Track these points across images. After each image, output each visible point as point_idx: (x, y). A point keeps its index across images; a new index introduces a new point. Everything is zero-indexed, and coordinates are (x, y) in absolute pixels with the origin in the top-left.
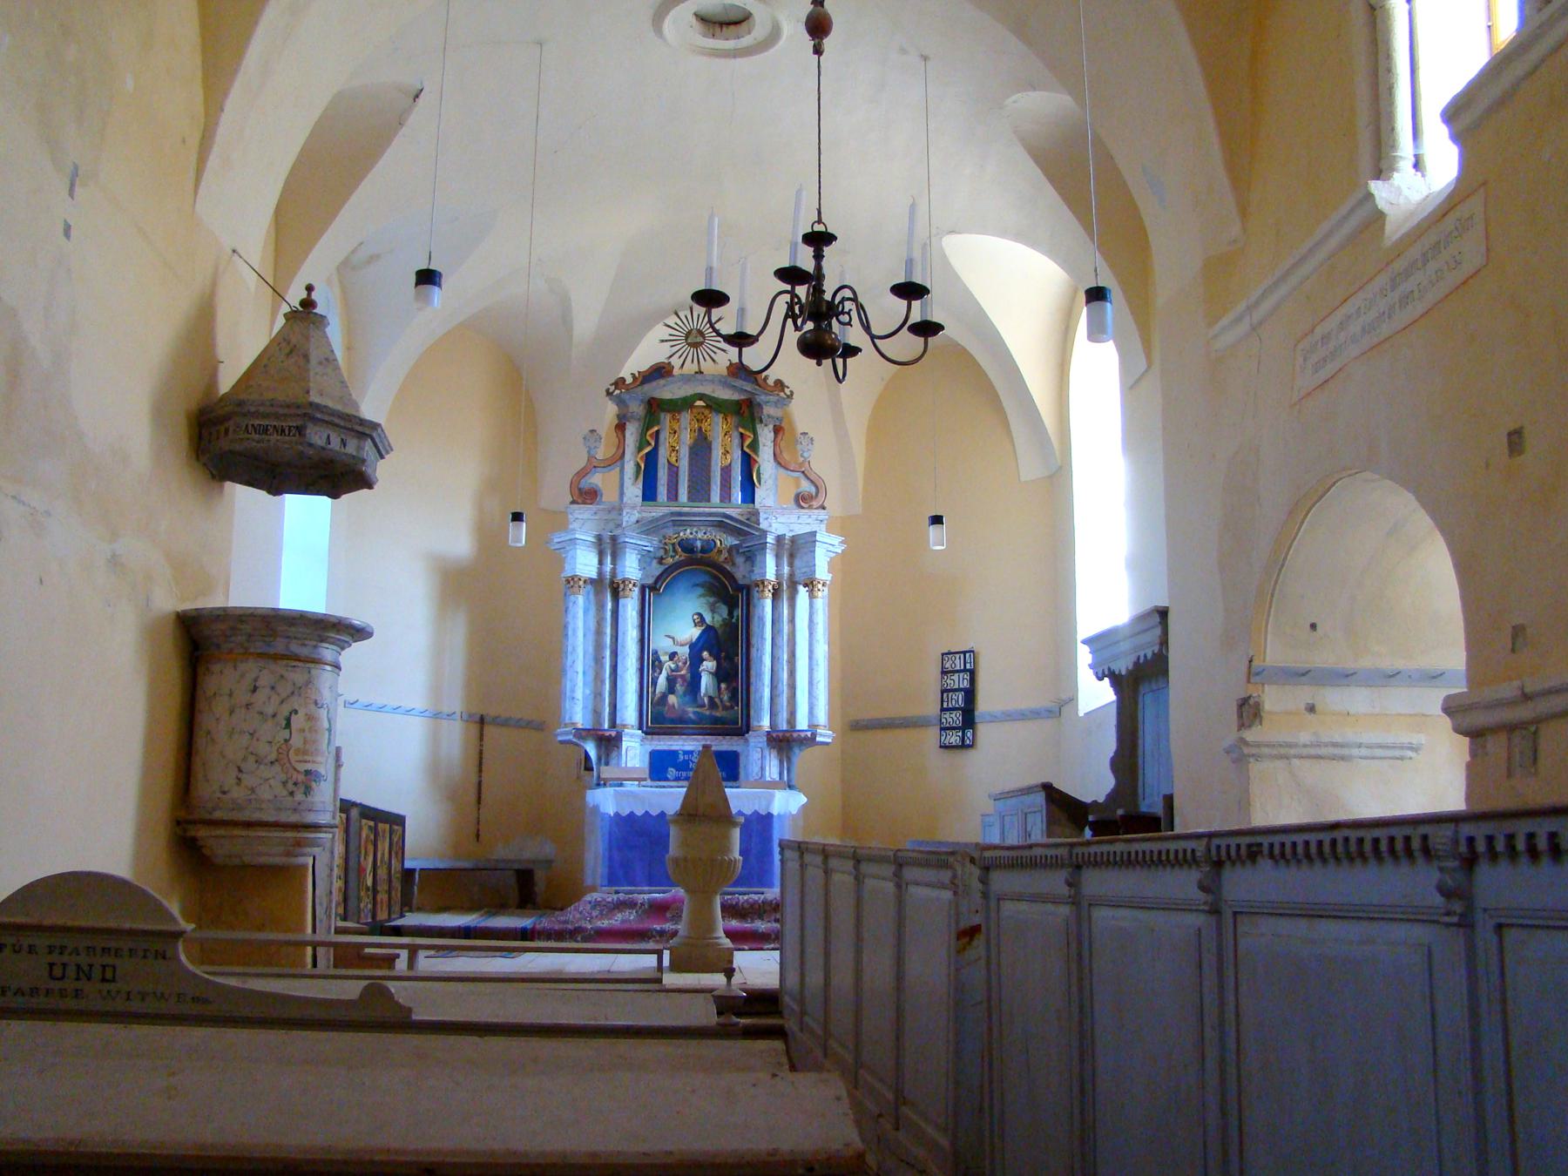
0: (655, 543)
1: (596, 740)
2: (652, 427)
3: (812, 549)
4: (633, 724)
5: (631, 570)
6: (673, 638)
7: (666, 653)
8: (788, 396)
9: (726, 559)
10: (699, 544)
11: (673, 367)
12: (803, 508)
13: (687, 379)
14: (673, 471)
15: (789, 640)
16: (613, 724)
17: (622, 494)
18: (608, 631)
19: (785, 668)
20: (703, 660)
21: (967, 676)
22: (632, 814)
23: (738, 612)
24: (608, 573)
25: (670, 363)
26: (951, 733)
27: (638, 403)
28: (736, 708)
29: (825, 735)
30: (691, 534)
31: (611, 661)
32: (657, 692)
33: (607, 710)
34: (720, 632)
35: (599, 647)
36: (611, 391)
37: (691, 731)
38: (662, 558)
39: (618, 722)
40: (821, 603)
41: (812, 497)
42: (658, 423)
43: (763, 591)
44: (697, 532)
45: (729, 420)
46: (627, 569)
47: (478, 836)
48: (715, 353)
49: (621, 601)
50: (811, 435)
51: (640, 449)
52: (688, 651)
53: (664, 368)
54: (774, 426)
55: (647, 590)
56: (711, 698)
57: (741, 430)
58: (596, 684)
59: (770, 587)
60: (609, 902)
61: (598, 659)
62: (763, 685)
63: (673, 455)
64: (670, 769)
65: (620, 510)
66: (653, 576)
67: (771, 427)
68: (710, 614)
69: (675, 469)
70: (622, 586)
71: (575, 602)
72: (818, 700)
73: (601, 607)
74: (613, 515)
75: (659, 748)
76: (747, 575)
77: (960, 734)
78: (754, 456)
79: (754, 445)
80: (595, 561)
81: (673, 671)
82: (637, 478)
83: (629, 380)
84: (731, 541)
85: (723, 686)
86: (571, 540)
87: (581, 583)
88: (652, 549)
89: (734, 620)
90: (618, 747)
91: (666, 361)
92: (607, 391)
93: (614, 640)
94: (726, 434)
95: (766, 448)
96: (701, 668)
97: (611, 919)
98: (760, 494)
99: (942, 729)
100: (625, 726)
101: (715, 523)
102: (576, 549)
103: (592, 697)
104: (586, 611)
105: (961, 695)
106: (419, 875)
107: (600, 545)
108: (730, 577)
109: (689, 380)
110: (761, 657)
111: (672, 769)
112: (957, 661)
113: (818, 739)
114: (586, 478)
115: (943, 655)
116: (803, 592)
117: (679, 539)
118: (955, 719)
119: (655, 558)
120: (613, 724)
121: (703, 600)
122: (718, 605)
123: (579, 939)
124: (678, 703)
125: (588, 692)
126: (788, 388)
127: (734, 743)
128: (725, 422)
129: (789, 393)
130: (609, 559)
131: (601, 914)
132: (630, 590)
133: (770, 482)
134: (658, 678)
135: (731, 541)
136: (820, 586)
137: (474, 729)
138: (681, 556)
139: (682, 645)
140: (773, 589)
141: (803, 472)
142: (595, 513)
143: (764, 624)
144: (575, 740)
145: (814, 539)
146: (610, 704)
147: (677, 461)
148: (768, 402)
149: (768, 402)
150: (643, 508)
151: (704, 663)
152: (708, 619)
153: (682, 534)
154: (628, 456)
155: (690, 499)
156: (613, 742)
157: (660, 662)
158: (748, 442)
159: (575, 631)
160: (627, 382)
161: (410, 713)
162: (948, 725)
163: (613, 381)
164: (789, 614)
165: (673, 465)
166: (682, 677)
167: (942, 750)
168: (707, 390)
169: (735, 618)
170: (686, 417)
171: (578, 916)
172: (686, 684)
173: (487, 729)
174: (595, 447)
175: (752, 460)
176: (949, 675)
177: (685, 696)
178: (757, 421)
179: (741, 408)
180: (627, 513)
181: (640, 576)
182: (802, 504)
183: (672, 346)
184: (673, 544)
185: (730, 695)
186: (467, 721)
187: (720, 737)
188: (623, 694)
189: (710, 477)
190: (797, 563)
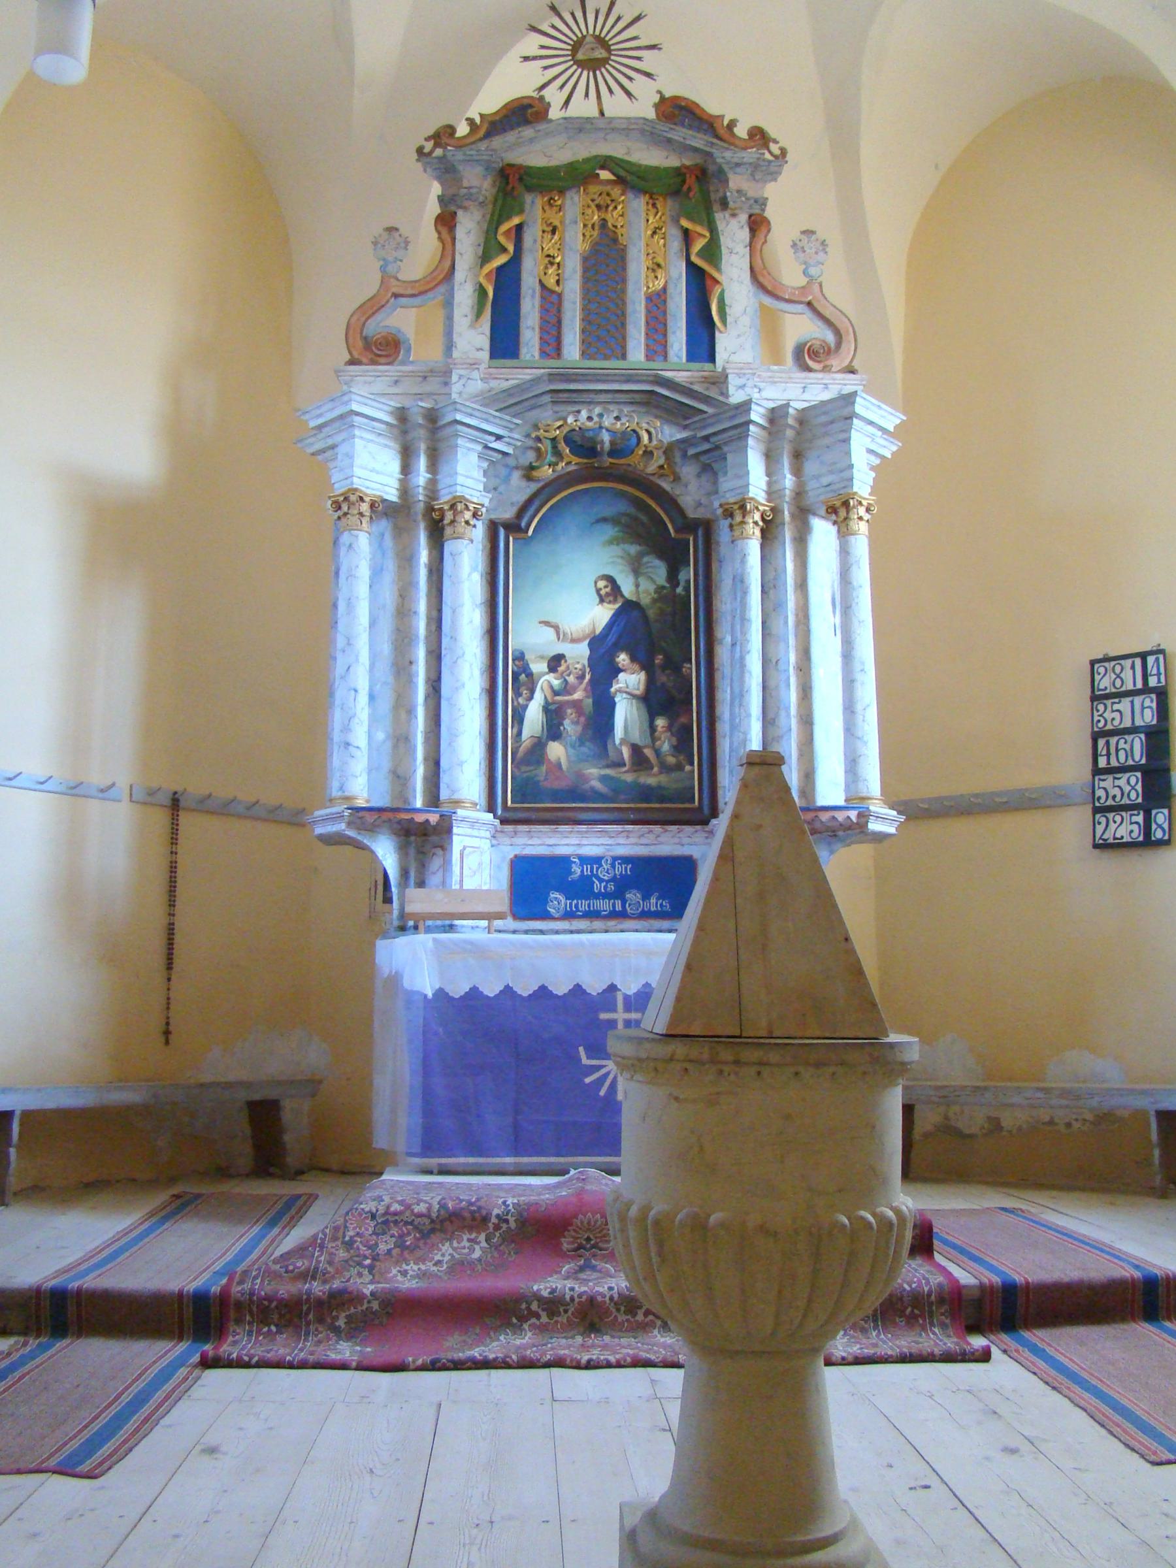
0: (516, 436)
1: (395, 833)
2: (509, 218)
3: (842, 436)
4: (476, 798)
5: (469, 483)
6: (556, 628)
7: (542, 657)
8: (776, 157)
9: (661, 467)
10: (606, 437)
11: (549, 104)
12: (809, 370)
13: (579, 127)
14: (552, 301)
15: (798, 624)
16: (433, 799)
17: (449, 347)
18: (422, 606)
19: (793, 680)
20: (620, 670)
21: (1150, 702)
22: (474, 993)
23: (688, 574)
24: (421, 490)
25: (542, 98)
26: (1118, 819)
27: (479, 169)
28: (688, 768)
29: (885, 821)
30: (590, 418)
31: (428, 670)
32: (526, 733)
33: (420, 771)
34: (651, 613)
35: (402, 639)
36: (426, 150)
37: (597, 816)
38: (532, 468)
39: (444, 794)
40: (861, 546)
41: (829, 349)
42: (521, 211)
43: (743, 523)
44: (601, 416)
45: (658, 206)
46: (460, 480)
47: (167, 1033)
48: (630, 79)
49: (449, 547)
50: (821, 235)
51: (485, 259)
52: (587, 652)
53: (531, 106)
54: (750, 216)
55: (502, 532)
56: (636, 750)
57: (685, 223)
58: (396, 720)
59: (757, 516)
60: (420, 1215)
61: (402, 668)
62: (749, 716)
63: (550, 271)
64: (554, 895)
65: (447, 373)
66: (512, 504)
67: (743, 218)
69: (555, 297)
70: (449, 516)
71: (350, 546)
72: (866, 743)
73: (406, 560)
74: (433, 385)
75: (529, 851)
77: (1140, 818)
78: (715, 274)
79: (712, 251)
80: (395, 466)
81: (556, 693)
82: (479, 314)
83: (462, 130)
84: (669, 433)
85: (660, 722)
86: (342, 417)
87: (365, 507)
88: (510, 451)
89: (679, 590)
90: (442, 848)
91: (535, 95)
92: (420, 151)
93: (434, 628)
94: (654, 233)
96: (613, 690)
97: (422, 1260)
98: (725, 344)
99: (1096, 810)
100: (457, 803)
101: (638, 397)
102: (353, 437)
103: (389, 745)
104: (376, 573)
105: (1138, 744)
106: (22, 1125)
107: (405, 432)
108: (671, 503)
109: (580, 130)
110: (742, 659)
111: (557, 895)
112: (1127, 675)
113: (874, 826)
114: (379, 316)
115: (1093, 663)
116: (822, 531)
117: (566, 430)
118: (1127, 789)
119: (517, 468)
120: (433, 799)
121: (616, 550)
122: (645, 559)
123: (341, 1322)
124: (568, 756)
125: (380, 736)
126: (775, 142)
127: (686, 840)
128: (653, 211)
129: (777, 152)
130: (422, 463)
131: (401, 1245)
132: (467, 523)
133: (746, 321)
134: (525, 707)
135: (669, 433)
136: (862, 511)
137: (161, 818)
138: (570, 463)
139: (574, 641)
140: (763, 519)
141: (809, 304)
142: (396, 382)
143: (745, 592)
144: (351, 833)
145: (846, 412)
146: (426, 759)
147: (558, 282)
148: (738, 165)
149: (738, 165)
150: (491, 370)
151: (621, 676)
152: (627, 588)
153: (570, 420)
154: (460, 275)
155: (584, 354)
156: (434, 839)
157: (530, 675)
158: (698, 245)
159: (350, 606)
160: (459, 134)
161: (13, 783)
162: (1110, 802)
163: (431, 132)
164: (795, 570)
165: (553, 292)
166: (577, 705)
167: (1097, 851)
168: (616, 148)
169: (682, 584)
170: (574, 203)
171: (342, 1254)
172: (582, 719)
173: (184, 819)
174: (396, 259)
175: (709, 282)
176: (1109, 702)
177: (582, 744)
178: (716, 207)
179: (684, 182)
180: (460, 377)
181: (486, 502)
182: (810, 363)
183: (545, 68)
184: (554, 440)
185: (674, 740)
186: (145, 803)
187: (657, 829)
188: (454, 736)
189: (624, 314)
190: (811, 467)
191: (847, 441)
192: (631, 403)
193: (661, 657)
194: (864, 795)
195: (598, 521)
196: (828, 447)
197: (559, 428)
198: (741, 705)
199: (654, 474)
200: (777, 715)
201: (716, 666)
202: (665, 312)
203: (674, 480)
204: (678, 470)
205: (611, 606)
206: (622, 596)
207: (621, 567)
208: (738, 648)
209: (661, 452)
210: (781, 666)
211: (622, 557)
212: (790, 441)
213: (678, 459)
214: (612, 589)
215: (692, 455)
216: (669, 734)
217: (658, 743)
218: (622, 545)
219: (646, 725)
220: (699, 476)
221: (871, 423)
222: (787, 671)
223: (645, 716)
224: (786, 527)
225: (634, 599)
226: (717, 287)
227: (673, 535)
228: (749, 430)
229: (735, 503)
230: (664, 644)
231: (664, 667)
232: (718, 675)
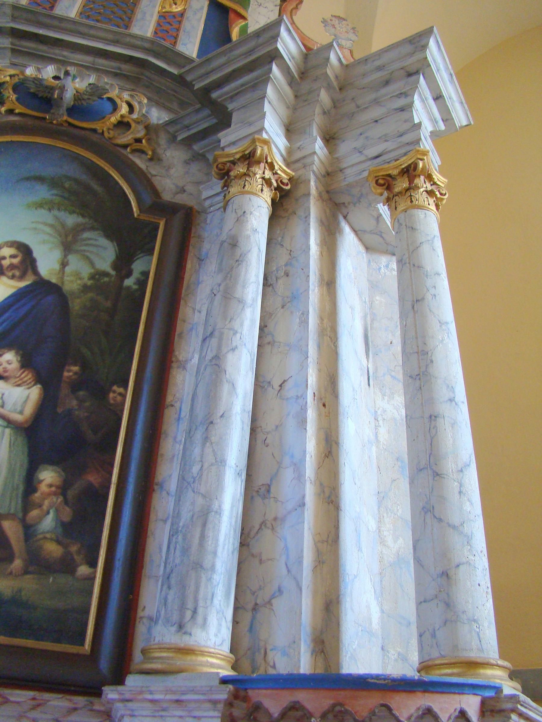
3: (401, 102)
15: (321, 333)
19: (311, 414)
28: (83, 570)
34: (76, 305)
62: (221, 462)
68: (57, 254)
76: (189, 188)
89: (129, 282)
95: (261, 9)
121: (44, 215)
122: (86, 235)
169: (136, 274)
175: (232, 16)
185: (67, 514)
191: (407, 108)
192: (116, 75)
193: (76, 369)
194: (473, 655)
195: (28, 179)
196: (376, 121)
197: (11, 76)
198: (206, 439)
199: (125, 147)
200: (275, 476)
201: (169, 399)
202: (178, 30)
203: (151, 160)
204: (160, 151)
205: (13, 283)
206: (35, 272)
207: (47, 238)
208: (214, 342)
209: (141, 127)
210: (290, 391)
211: (51, 226)
212: (324, 113)
213: (163, 139)
214: (23, 262)
215: (183, 140)
216: (61, 499)
217: (34, 513)
218: (56, 212)
219: (19, 479)
220: (187, 162)
221: (438, 98)
222: (303, 396)
223: (22, 459)
224: (312, 197)
225: (54, 281)
226: (241, 21)
227: (136, 215)
228: (271, 69)
229: (236, 153)
230: (87, 353)
231: (75, 387)
232: (170, 415)
